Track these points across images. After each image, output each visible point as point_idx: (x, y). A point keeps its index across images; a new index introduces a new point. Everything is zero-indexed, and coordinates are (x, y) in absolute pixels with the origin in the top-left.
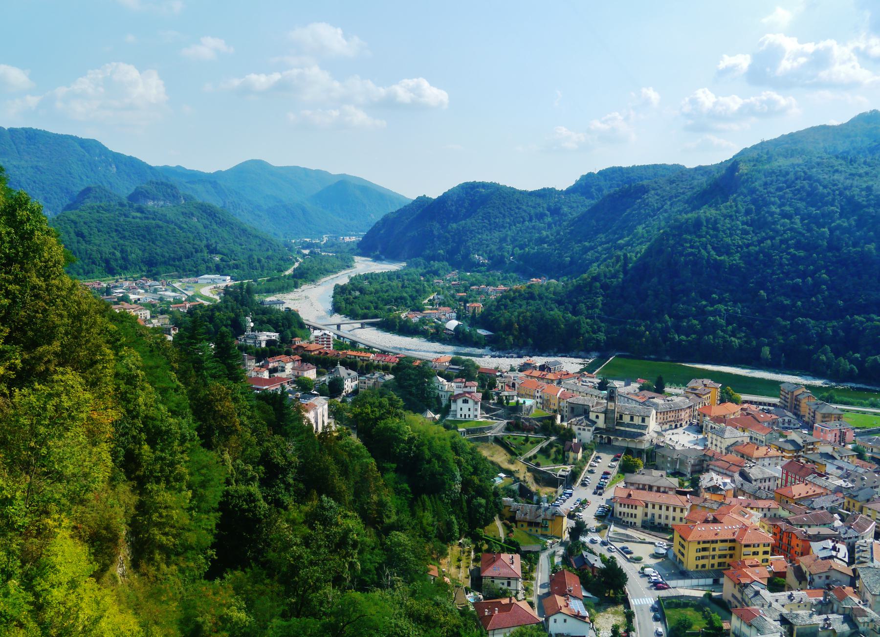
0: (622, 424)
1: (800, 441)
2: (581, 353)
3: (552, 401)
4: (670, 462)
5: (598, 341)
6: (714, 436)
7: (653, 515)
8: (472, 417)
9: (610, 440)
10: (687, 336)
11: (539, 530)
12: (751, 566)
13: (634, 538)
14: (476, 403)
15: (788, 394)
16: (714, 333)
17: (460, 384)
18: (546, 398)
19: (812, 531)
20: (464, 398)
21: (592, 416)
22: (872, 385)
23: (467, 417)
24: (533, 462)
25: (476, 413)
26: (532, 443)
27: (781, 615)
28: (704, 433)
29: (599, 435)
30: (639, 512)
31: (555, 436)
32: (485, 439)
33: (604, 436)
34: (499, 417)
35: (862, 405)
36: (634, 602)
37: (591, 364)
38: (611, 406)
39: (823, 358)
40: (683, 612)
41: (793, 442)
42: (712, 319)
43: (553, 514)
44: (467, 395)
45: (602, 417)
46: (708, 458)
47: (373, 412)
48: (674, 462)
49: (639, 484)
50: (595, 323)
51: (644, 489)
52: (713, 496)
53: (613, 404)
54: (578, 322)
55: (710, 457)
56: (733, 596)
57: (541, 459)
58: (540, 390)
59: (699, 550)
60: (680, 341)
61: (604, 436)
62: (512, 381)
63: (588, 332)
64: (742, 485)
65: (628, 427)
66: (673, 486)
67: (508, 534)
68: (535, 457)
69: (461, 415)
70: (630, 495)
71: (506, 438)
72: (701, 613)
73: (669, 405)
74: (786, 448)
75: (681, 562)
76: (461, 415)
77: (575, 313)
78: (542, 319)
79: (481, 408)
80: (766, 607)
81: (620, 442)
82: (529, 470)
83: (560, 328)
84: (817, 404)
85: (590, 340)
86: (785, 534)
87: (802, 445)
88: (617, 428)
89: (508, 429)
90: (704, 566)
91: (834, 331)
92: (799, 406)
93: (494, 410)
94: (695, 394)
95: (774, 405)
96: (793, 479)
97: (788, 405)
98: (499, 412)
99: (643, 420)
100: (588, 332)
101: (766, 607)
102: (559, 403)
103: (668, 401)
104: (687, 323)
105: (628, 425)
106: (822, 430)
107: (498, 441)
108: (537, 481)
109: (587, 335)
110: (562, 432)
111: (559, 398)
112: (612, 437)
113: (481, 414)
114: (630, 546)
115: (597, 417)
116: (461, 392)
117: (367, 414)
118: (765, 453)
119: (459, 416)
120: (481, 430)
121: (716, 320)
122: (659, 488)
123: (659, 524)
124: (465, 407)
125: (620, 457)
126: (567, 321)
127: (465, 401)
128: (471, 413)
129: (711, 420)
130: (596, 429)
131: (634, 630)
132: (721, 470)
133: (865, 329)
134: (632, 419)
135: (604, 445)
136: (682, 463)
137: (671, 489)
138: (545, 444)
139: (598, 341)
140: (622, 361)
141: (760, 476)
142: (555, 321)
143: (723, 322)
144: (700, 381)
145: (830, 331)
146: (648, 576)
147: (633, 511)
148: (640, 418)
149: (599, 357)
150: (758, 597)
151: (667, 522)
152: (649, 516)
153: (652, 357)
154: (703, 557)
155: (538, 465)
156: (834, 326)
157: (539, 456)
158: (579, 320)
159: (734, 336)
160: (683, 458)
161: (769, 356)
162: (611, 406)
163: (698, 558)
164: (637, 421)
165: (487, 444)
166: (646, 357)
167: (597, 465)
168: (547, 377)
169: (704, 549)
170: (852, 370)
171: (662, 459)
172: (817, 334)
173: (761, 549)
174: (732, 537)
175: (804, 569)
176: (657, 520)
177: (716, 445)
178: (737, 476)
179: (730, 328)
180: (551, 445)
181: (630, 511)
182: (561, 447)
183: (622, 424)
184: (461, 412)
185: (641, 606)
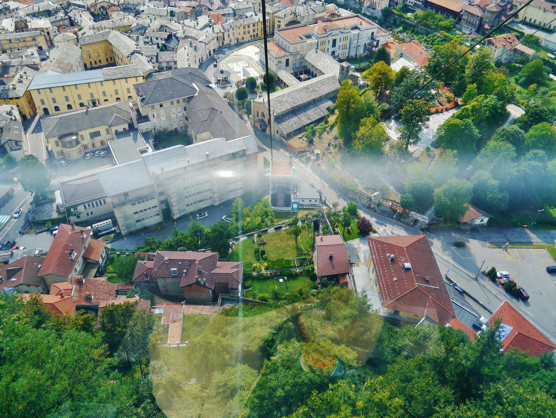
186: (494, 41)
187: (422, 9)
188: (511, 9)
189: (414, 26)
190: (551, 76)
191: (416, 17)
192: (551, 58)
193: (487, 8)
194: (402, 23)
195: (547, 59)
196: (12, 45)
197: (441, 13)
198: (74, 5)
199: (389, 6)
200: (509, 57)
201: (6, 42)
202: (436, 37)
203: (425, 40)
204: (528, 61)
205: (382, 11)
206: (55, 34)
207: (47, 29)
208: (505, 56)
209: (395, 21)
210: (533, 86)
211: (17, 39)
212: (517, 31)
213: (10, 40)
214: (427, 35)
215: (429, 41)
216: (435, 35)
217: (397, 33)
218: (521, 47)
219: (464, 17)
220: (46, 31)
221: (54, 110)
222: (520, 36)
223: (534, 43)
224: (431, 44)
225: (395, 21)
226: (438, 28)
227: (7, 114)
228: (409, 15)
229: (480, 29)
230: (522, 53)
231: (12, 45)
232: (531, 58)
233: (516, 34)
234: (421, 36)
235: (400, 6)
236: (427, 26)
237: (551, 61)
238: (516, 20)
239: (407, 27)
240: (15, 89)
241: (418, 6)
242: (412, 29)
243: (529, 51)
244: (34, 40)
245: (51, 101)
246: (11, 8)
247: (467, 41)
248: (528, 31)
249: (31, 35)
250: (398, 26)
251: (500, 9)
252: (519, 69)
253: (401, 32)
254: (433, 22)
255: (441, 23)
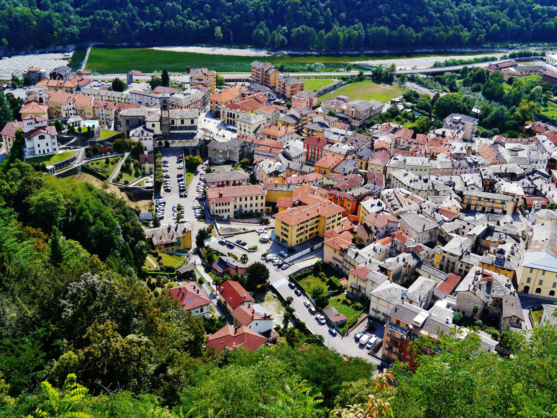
0: (175, 128)
1: (298, 115)
2: (60, 48)
3: (86, 111)
4: (222, 154)
5: (71, 33)
6: (243, 124)
7: (241, 206)
8: (51, 151)
9: (167, 144)
10: (152, 23)
11: (174, 248)
12: (340, 233)
13: (238, 230)
14: (53, 137)
15: (259, 71)
16: (173, 17)
17: (30, 121)
18: (79, 108)
19: (357, 192)
20: (40, 135)
21: (149, 126)
22: (297, 51)
23: (46, 152)
24: (122, 181)
25: (54, 147)
26: (112, 163)
27: (379, 266)
28: (221, 118)
29: (158, 142)
30: (231, 207)
31: (128, 152)
32: (74, 172)
33: (163, 141)
34: (75, 145)
35: (304, 71)
36: (276, 285)
37: (73, 58)
38: (165, 114)
39: (261, 32)
40: (306, 281)
41: (293, 116)
42: (170, 4)
43: (184, 232)
44: (42, 131)
45: (158, 125)
46: (248, 144)
47: (11, 186)
48: (224, 153)
49: (219, 182)
50: (65, 16)
51: (223, 185)
52: (276, 179)
53: (167, 112)
54: (49, 17)
55: (250, 144)
56: (334, 258)
57: (126, 177)
58: (71, 102)
59: (298, 230)
60: (147, 27)
61: (163, 141)
62: (39, 96)
63: (60, 26)
64: (289, 164)
65: (181, 130)
66: (245, 178)
67: (158, 261)
68: (121, 176)
69: (40, 151)
70: (221, 195)
71: (90, 164)
72: (319, 278)
73: (189, 98)
74: (290, 122)
75: (286, 242)
76: (40, 151)
77: (43, 7)
78: (10, 16)
79: (58, 142)
80: (368, 262)
81: (177, 144)
82: (122, 190)
83: (33, 25)
84: (285, 78)
85: (64, 33)
86: (339, 199)
87: (299, 118)
88: (172, 132)
89: (88, 155)
90: (301, 240)
91: (265, 9)
92: (268, 79)
93: (69, 139)
94: (201, 84)
95: (247, 80)
96: (313, 150)
97: (260, 79)
98: (73, 141)
99: (192, 122)
100: (60, 26)
101: (368, 262)
102: (94, 111)
103: (185, 94)
104: (149, 10)
105: (181, 128)
106: (299, 100)
107: (85, 169)
108: (131, 199)
109: (60, 30)
110: (133, 147)
111: (94, 107)
112: (170, 141)
113: (59, 145)
114: (243, 238)
115: (153, 125)
116: (33, 128)
117: (7, 190)
118: (285, 131)
119: (37, 152)
120: (68, 163)
121: (173, 6)
122: (234, 182)
123: (246, 211)
124: (43, 142)
125: (182, 157)
126: (37, 16)
127: (42, 137)
128: (50, 148)
129: (227, 107)
130: (155, 136)
131: (294, 310)
132: (264, 154)
133: (287, 6)
134: (182, 122)
135: (167, 150)
136: (231, 152)
137: (244, 180)
138: (122, 162)
139: (73, 35)
140: (101, 52)
141: (297, 154)
142: (25, 18)
143: (180, 7)
144: (199, 70)
145: (262, 9)
146: (270, 260)
147: (227, 207)
148: (190, 120)
149: (76, 49)
150: (358, 257)
151: (251, 209)
152: (238, 207)
153: (125, 44)
154: (302, 234)
155: (126, 183)
156: (265, 5)
157: (124, 174)
158: (50, 15)
159: (191, 19)
160: (232, 149)
161: (221, 35)
162: (165, 114)
163: (298, 236)
164: (187, 123)
165: (77, 176)
166: (119, 45)
167: (168, 169)
168: (66, 85)
169: (301, 228)
170: (283, 39)
171: (213, 153)
172: (254, 12)
173: (336, 218)
174: (318, 214)
175: (369, 225)
176: (244, 209)
177: (245, 130)
178: (281, 157)
179: (186, 11)
180: (127, 161)
181: (224, 207)
182: (136, 161)
183: (175, 128)
184: (39, 149)
185: (281, 287)
196: (479, 203)
198: (540, 173)
201: (476, 198)
206: (538, 208)
207: (518, 196)
211: (487, 199)
213: (480, 198)
220: (516, 197)
221: (535, 290)
227: (506, 286)
231: (479, 203)
240: (509, 260)
244: (503, 203)
245: (538, 282)
246: (479, 163)
249: (502, 198)
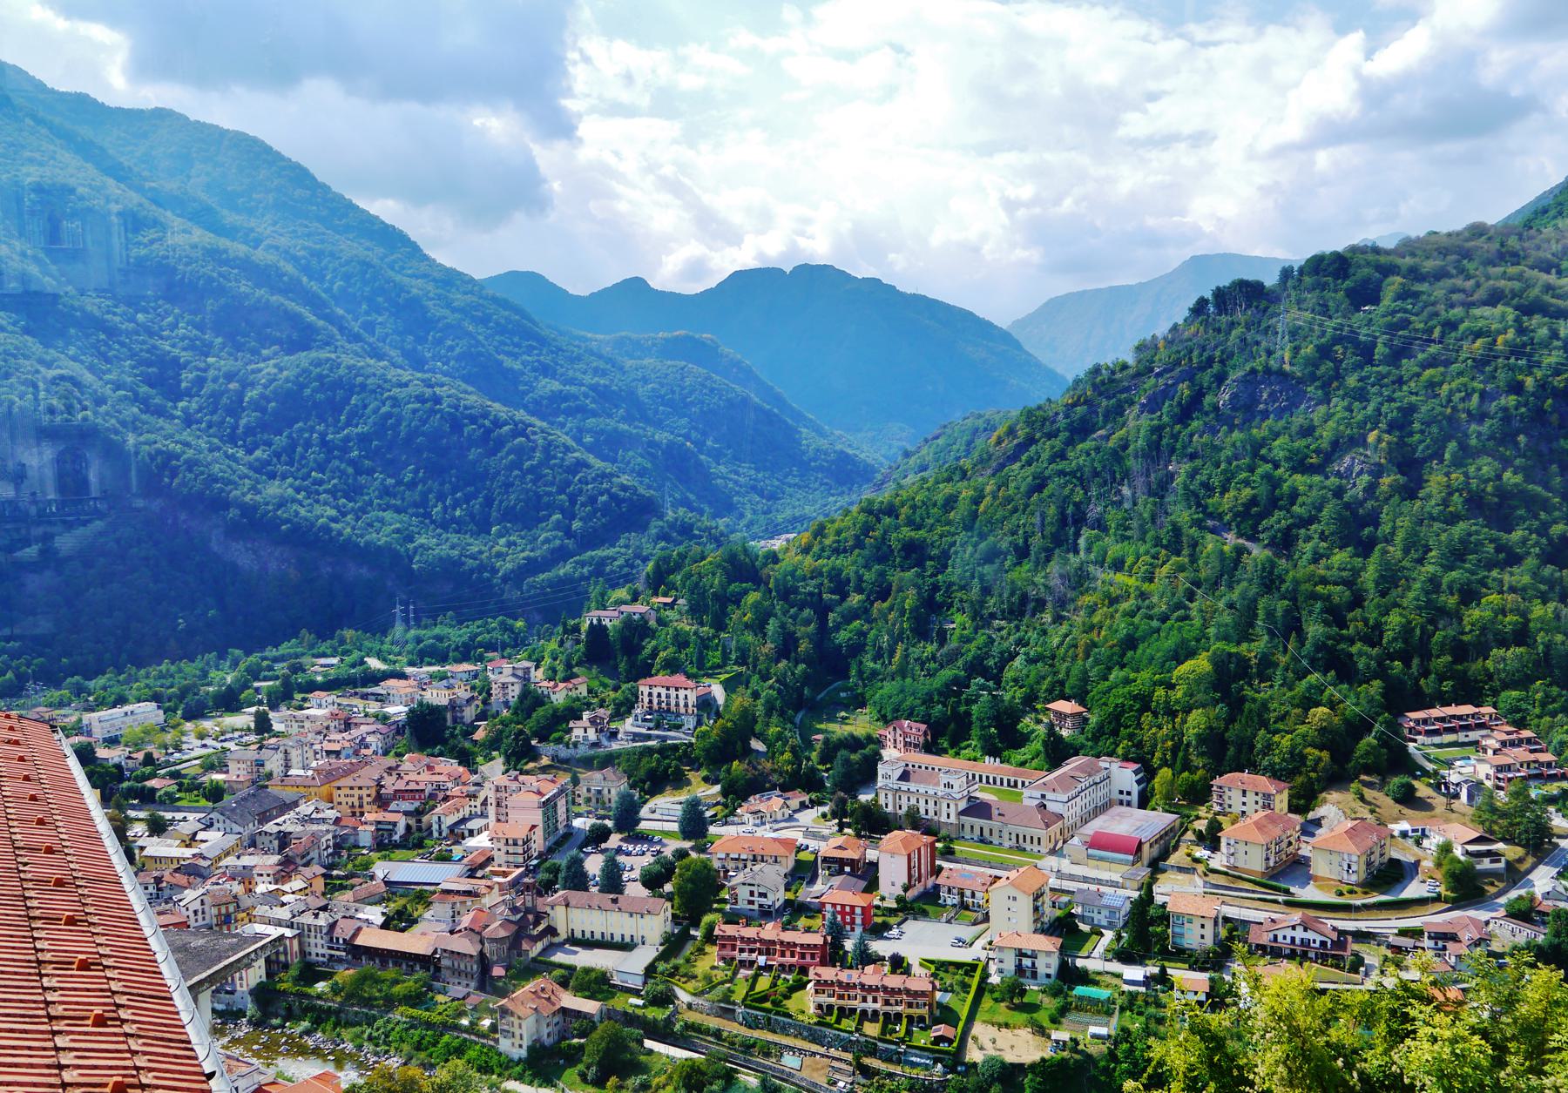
186: (511, 1006)
187: (350, 965)
188: (537, 923)
189: (338, 1012)
190: (648, 1043)
191: (336, 990)
192: (637, 1006)
193: (486, 933)
194: (306, 1011)
195: (630, 1010)
197: (396, 964)
199: (269, 974)
200: (556, 1029)
202: (390, 1026)
203: (370, 1038)
204: (594, 1027)
205: (252, 992)
208: (545, 1031)
209: (289, 1009)
210: (613, 1080)
212: (561, 966)
214: (370, 1025)
215: (378, 1038)
216: (388, 1021)
217: (301, 1037)
218: (570, 1001)
219: (445, 962)
222: (569, 978)
223: (597, 985)
224: (386, 1043)
225: (289, 1009)
226: (390, 1003)
228: (321, 986)
229: (485, 982)
230: (578, 1014)
232: (596, 1019)
233: (558, 972)
234: (357, 1029)
235: (294, 972)
236: (368, 1002)
237: (639, 1012)
238: (556, 940)
239: (320, 1017)
241: (340, 960)
242: (333, 1019)
243: (590, 1006)
247: (462, 1014)
248: (584, 959)
250: (300, 1019)
251: (514, 928)
252: (581, 1047)
253: (308, 1032)
254: (380, 991)
255: (397, 989)
